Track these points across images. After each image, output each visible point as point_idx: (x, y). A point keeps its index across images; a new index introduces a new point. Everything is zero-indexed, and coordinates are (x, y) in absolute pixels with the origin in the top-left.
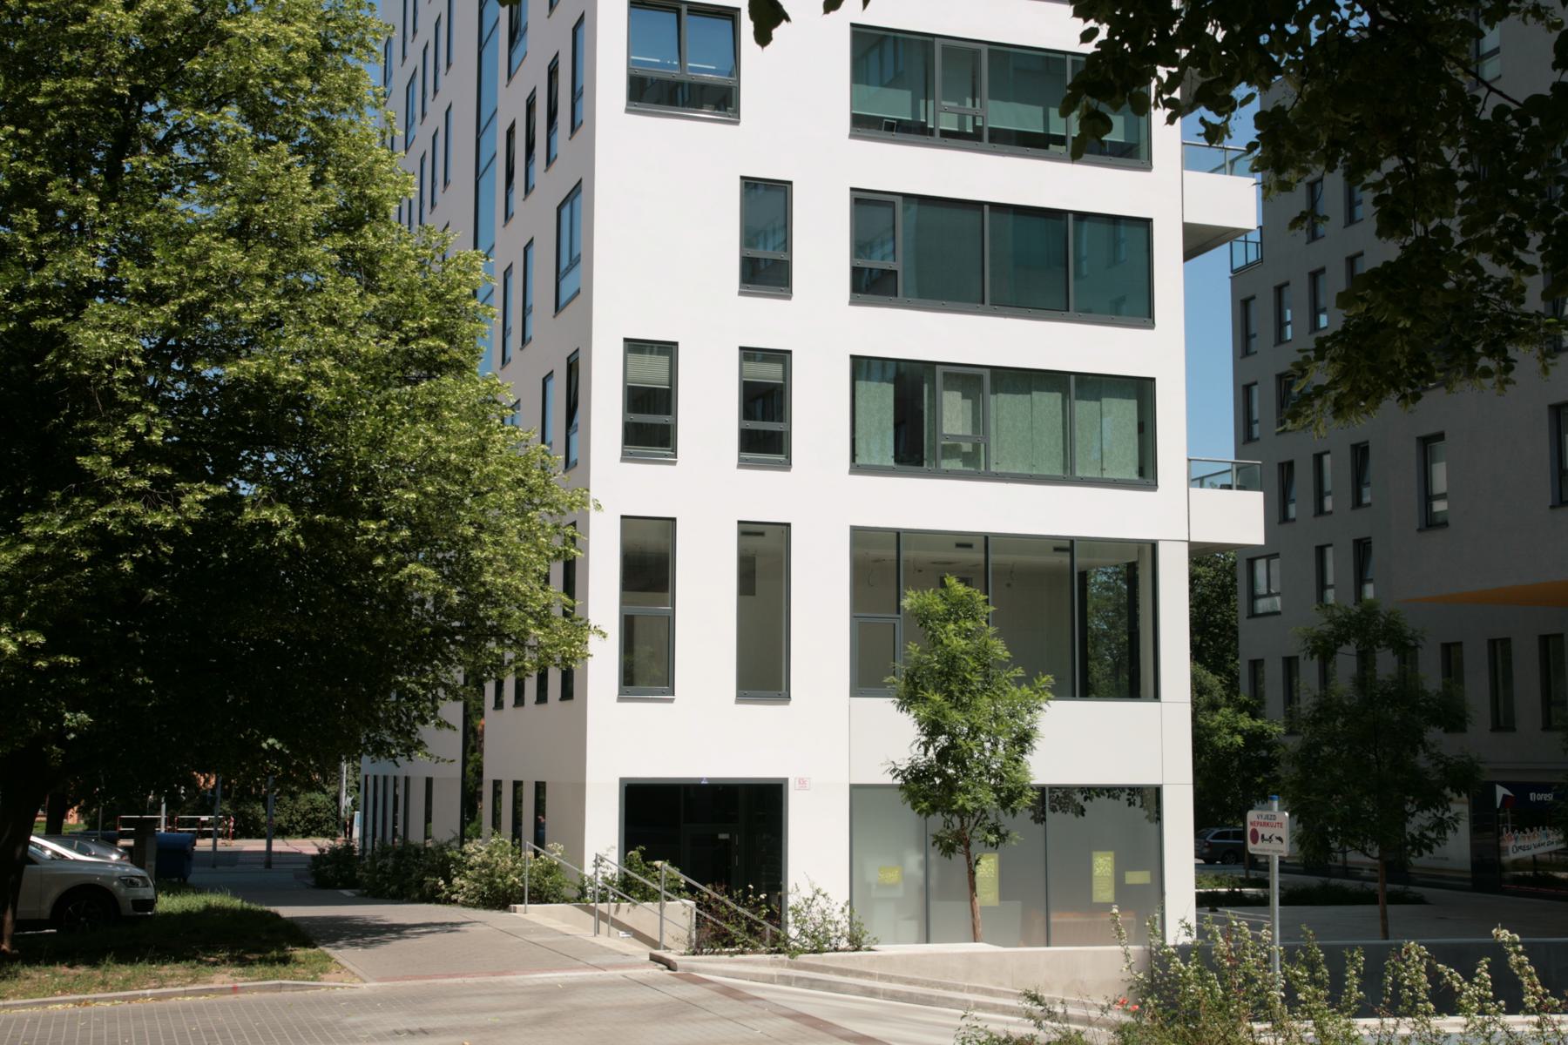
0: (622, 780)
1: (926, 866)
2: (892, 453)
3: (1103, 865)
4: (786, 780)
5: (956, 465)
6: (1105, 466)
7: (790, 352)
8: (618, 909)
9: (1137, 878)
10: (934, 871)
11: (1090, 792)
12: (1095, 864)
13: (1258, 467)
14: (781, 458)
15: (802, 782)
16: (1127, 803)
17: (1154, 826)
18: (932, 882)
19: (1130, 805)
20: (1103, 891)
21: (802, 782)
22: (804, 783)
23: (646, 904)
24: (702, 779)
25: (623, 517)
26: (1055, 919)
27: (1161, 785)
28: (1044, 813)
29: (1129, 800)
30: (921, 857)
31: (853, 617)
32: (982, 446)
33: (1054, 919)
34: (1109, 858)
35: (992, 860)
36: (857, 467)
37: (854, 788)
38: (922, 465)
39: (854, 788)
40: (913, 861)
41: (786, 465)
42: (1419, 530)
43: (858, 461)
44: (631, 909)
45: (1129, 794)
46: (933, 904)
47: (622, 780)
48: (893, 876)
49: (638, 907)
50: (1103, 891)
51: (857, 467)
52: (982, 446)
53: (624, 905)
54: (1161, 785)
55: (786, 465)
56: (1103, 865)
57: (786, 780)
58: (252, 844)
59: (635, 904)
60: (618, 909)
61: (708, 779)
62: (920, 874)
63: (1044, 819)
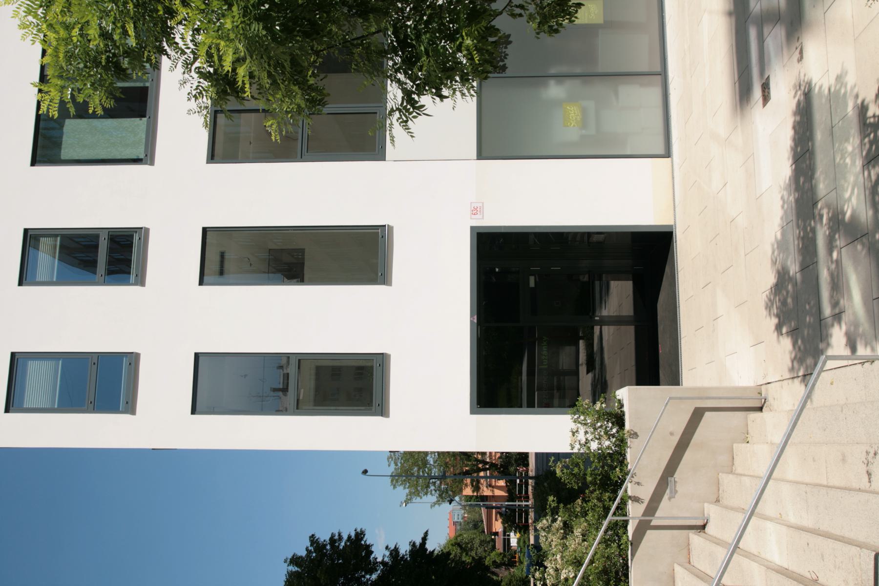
0: (473, 412)
1: (560, 77)
2: (137, 121)
4: (472, 228)
7: (26, 231)
8: (636, 499)
10: (564, 69)
14: (136, 238)
15: (475, 211)
18: (578, 70)
22: (476, 209)
24: (472, 322)
25: (194, 411)
30: (552, 82)
31: (302, 158)
36: (146, 158)
37: (481, 156)
38: (147, 88)
39: (481, 156)
40: (555, 91)
41: (143, 233)
43: (142, 156)
44: (635, 479)
46: (600, 69)
48: (573, 112)
51: (146, 158)
55: (143, 233)
57: (472, 228)
58: (532, 458)
60: (636, 499)
61: (472, 316)
62: (569, 83)
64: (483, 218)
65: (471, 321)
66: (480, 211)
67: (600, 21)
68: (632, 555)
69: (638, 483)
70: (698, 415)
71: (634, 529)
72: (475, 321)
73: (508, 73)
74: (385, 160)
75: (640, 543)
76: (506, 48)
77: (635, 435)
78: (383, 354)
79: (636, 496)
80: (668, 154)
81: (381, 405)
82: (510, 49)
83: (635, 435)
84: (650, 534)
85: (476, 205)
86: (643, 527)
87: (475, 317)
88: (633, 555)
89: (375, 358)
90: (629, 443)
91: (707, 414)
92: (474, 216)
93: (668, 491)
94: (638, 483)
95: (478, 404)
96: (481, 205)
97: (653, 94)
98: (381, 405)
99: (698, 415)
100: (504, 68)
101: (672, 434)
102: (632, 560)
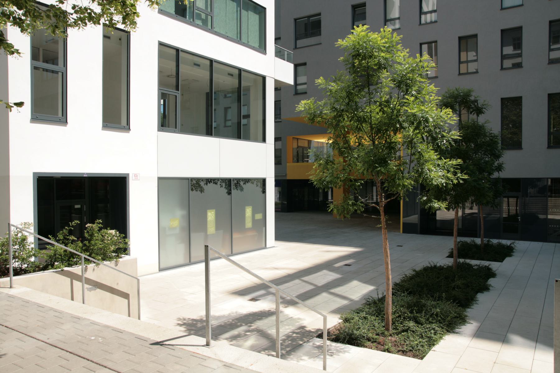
0: (35, 174)
2: (174, 10)
3: (249, 211)
4: (128, 174)
5: (199, 22)
6: (249, 41)
9: (259, 216)
11: (247, 181)
12: (246, 212)
13: (292, 54)
15: (136, 176)
16: (256, 185)
17: (264, 195)
19: (221, 187)
20: (249, 224)
21: (136, 176)
23: (105, 262)
24: (84, 174)
26: (235, 236)
27: (266, 178)
28: (231, 190)
29: (220, 184)
32: (209, 18)
33: (234, 236)
34: (250, 209)
35: (213, 213)
37: (160, 179)
39: (160, 179)
42: (294, 95)
44: (96, 268)
45: (221, 182)
46: (192, 235)
47: (35, 174)
49: (101, 266)
50: (249, 224)
52: (209, 18)
53: (91, 266)
54: (266, 178)
56: (249, 211)
57: (128, 174)
59: (98, 264)
60: (86, 270)
61: (87, 174)
63: (231, 193)
64: (133, 180)
65: (85, 173)
66: (136, 178)
67: (208, 233)
68: (56, 271)
69: (94, 270)
70: (126, 296)
71: (71, 271)
72: (85, 176)
73: (191, 192)
74: (158, 131)
75: (64, 275)
76: (200, 191)
77: (116, 265)
78: (67, 122)
79: (88, 270)
80: (161, 270)
81: (37, 118)
82: (199, 192)
83: (116, 265)
84: (68, 280)
85: (138, 176)
86: (73, 277)
87: (86, 176)
88: (56, 272)
89: (64, 117)
90: (113, 262)
91: (127, 301)
92: (134, 175)
93: (91, 287)
94: (94, 270)
95: (39, 177)
96: (139, 179)
97: (181, 259)
98: (37, 118)
99: (126, 296)
100: (192, 190)
101: (118, 284)
102: (53, 272)
